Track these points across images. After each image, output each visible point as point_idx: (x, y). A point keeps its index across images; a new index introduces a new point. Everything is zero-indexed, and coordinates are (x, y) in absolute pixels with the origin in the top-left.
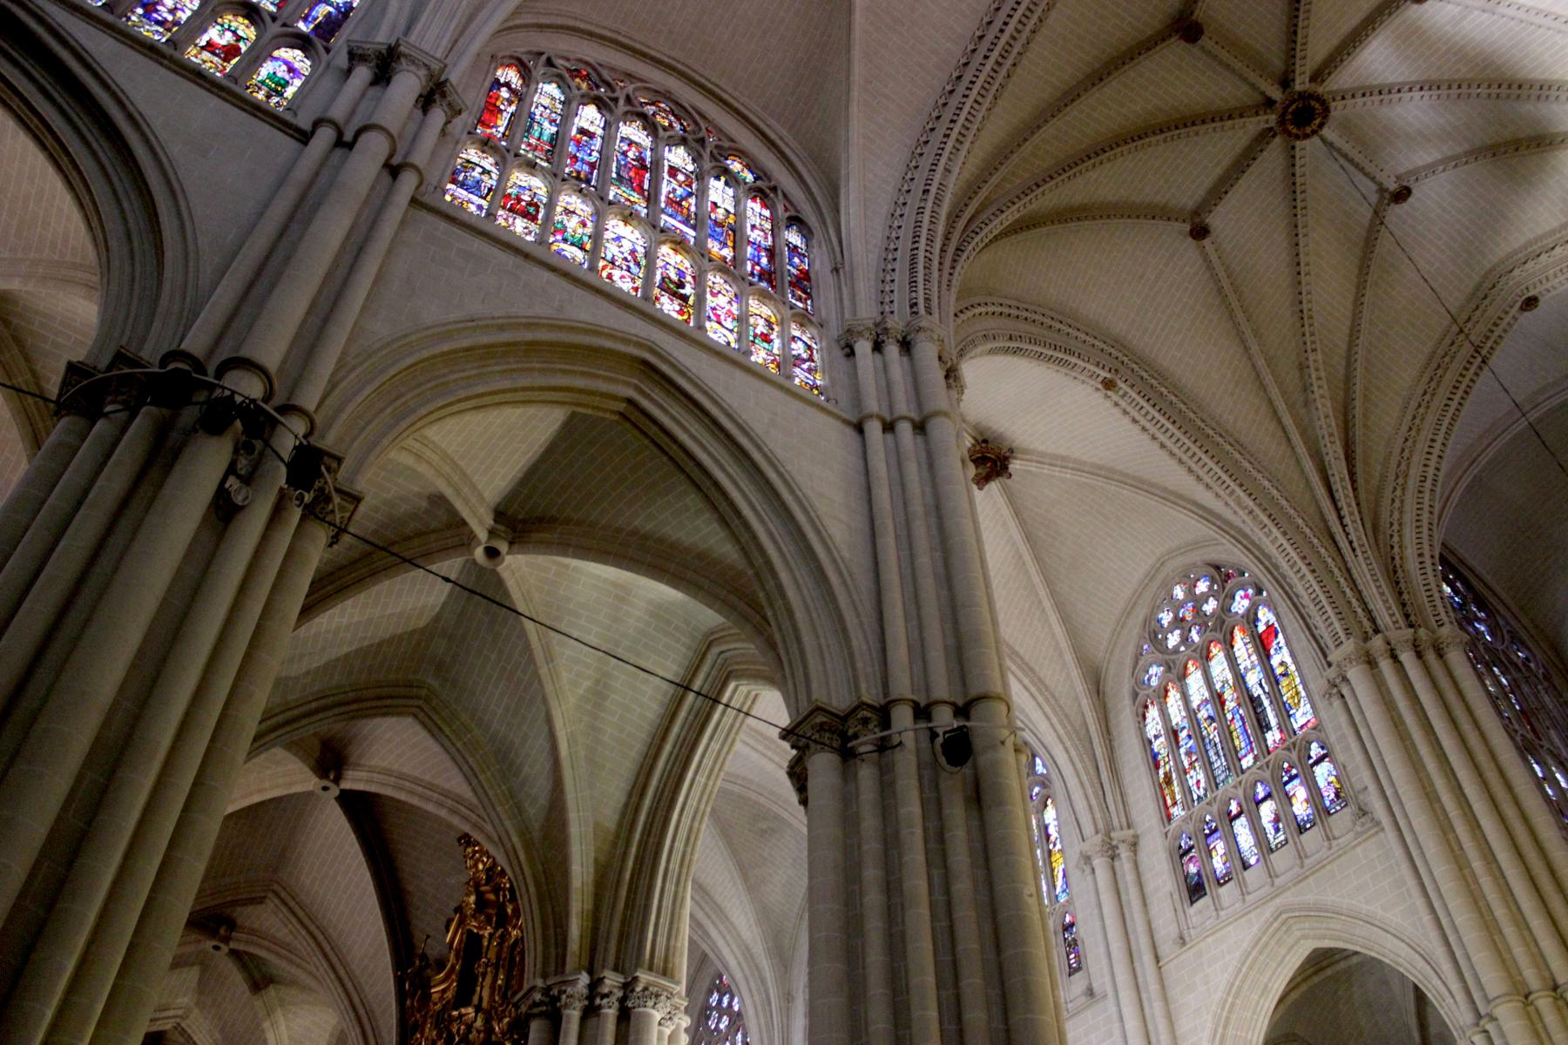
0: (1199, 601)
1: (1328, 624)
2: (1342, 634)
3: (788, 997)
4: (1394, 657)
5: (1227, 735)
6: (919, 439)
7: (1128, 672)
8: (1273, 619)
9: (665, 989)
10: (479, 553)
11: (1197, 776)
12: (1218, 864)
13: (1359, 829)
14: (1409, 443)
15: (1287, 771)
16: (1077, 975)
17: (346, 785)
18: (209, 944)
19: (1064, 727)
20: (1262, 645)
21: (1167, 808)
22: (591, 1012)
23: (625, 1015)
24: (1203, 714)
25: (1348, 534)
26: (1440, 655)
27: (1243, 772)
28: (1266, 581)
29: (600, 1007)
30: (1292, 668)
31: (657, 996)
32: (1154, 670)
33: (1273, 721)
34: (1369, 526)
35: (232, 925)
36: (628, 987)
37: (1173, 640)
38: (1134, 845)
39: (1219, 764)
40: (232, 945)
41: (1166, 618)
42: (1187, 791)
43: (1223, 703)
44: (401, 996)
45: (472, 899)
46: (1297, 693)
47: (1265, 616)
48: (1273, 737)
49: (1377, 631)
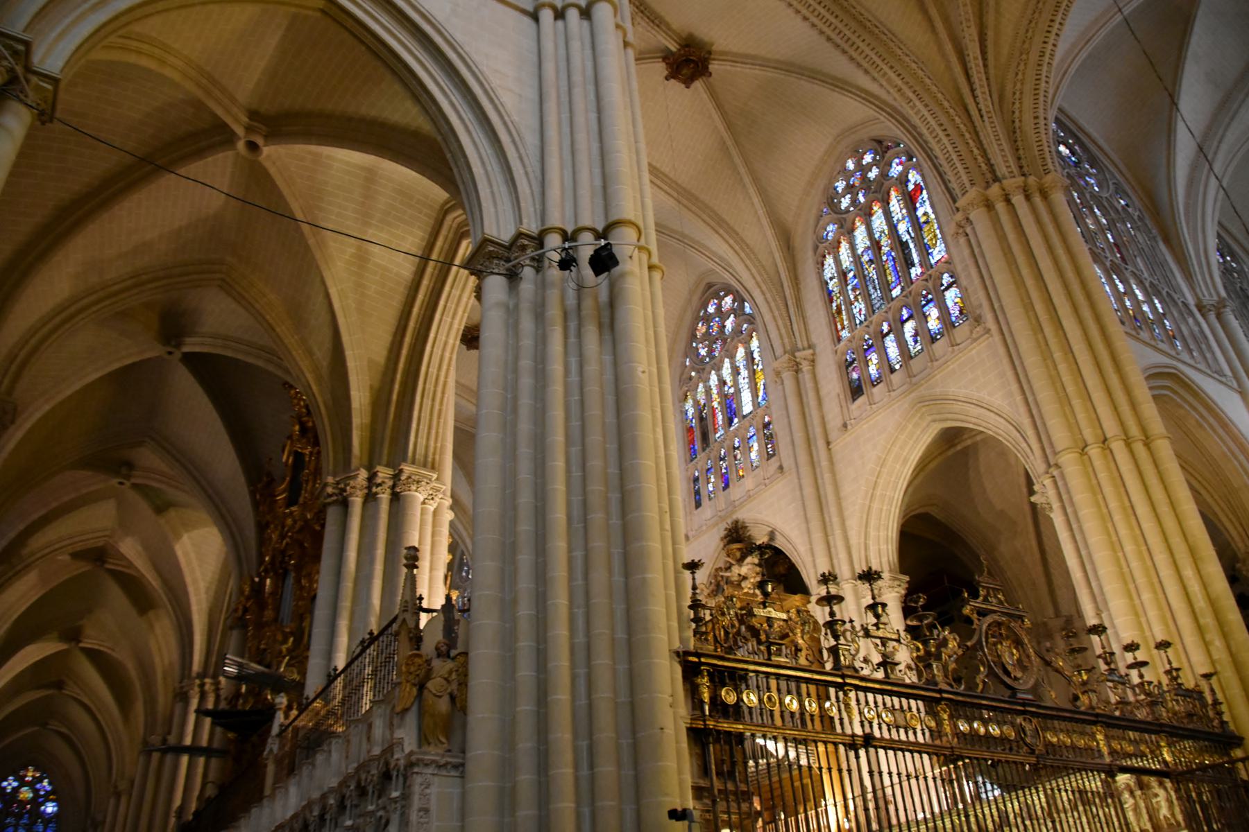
1: (958, 176)
2: (968, 185)
3: (434, 454)
4: (1008, 201)
5: (882, 272)
6: (585, 23)
7: (811, 231)
8: (919, 180)
9: (424, 476)
10: (241, 145)
11: (859, 307)
12: (873, 370)
13: (974, 336)
14: (1033, 25)
15: (925, 297)
16: (773, 459)
17: (186, 349)
18: (115, 481)
19: (761, 275)
20: (910, 201)
21: (837, 331)
22: (371, 498)
23: (396, 497)
24: (865, 258)
25: (977, 104)
26: (1045, 195)
27: (892, 299)
28: (915, 148)
29: (376, 493)
30: (933, 216)
31: (418, 482)
32: (830, 228)
33: (916, 260)
34: (995, 97)
35: (130, 465)
36: (396, 477)
37: (845, 202)
38: (813, 362)
39: (876, 295)
40: (133, 481)
41: (841, 185)
42: (852, 317)
43: (880, 248)
44: (256, 505)
45: (297, 428)
46: (935, 236)
47: (914, 177)
48: (916, 271)
49: (996, 179)
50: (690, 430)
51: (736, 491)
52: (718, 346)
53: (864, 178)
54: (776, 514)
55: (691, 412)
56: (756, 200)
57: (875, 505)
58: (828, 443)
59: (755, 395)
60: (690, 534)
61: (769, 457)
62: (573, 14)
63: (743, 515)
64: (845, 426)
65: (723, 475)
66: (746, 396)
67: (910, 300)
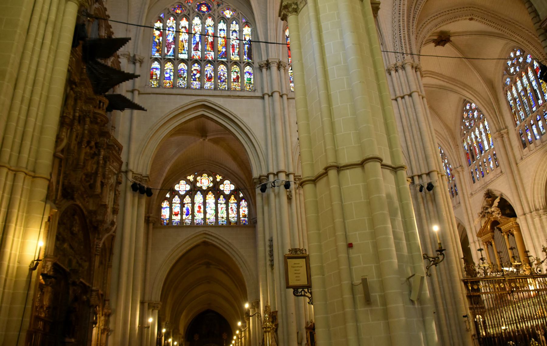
0: (518, 58)
6: (410, 98)
7: (501, 81)
11: (521, 113)
12: (529, 138)
15: (545, 112)
16: (498, 168)
19: (483, 102)
21: (515, 121)
24: (522, 94)
27: (533, 112)
32: (508, 80)
33: (540, 98)
37: (512, 70)
38: (508, 133)
39: (528, 109)
41: (509, 63)
42: (520, 117)
43: (527, 91)
48: (540, 102)
50: (467, 154)
51: (488, 178)
52: (472, 122)
53: (518, 62)
54: (502, 187)
55: (466, 147)
56: (477, 75)
57: (536, 187)
58: (517, 164)
59: (489, 143)
60: (473, 193)
61: (497, 166)
62: (407, 97)
63: (491, 187)
64: (522, 159)
65: (482, 172)
66: (486, 143)
67: (539, 113)
